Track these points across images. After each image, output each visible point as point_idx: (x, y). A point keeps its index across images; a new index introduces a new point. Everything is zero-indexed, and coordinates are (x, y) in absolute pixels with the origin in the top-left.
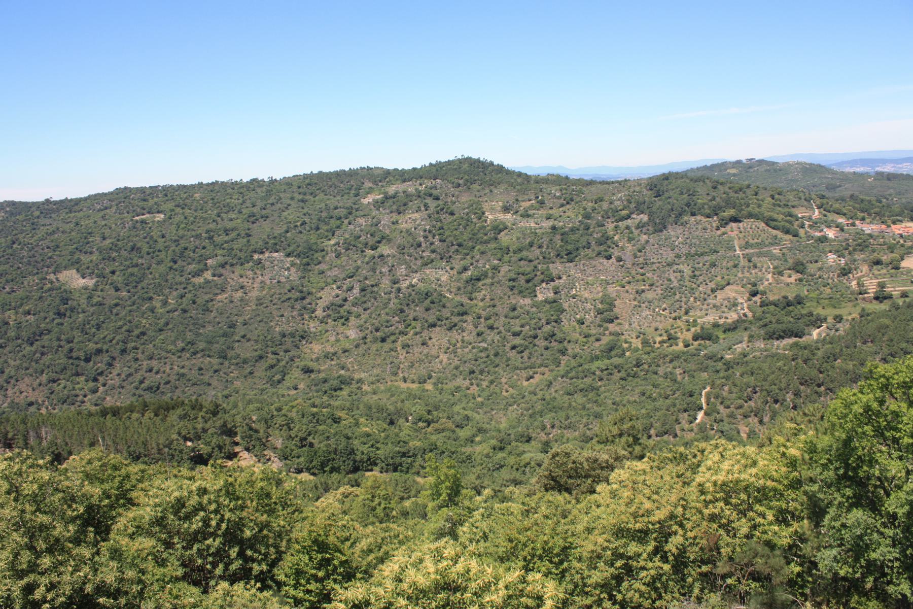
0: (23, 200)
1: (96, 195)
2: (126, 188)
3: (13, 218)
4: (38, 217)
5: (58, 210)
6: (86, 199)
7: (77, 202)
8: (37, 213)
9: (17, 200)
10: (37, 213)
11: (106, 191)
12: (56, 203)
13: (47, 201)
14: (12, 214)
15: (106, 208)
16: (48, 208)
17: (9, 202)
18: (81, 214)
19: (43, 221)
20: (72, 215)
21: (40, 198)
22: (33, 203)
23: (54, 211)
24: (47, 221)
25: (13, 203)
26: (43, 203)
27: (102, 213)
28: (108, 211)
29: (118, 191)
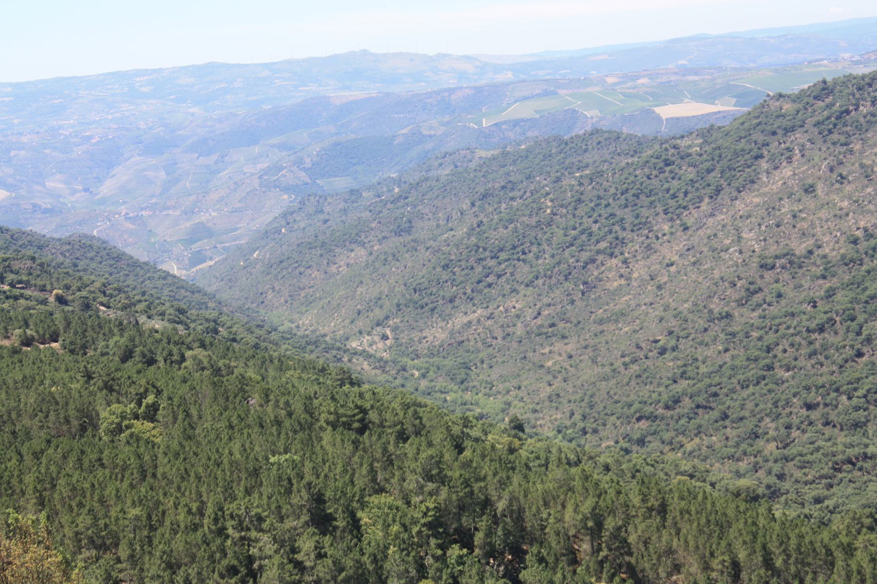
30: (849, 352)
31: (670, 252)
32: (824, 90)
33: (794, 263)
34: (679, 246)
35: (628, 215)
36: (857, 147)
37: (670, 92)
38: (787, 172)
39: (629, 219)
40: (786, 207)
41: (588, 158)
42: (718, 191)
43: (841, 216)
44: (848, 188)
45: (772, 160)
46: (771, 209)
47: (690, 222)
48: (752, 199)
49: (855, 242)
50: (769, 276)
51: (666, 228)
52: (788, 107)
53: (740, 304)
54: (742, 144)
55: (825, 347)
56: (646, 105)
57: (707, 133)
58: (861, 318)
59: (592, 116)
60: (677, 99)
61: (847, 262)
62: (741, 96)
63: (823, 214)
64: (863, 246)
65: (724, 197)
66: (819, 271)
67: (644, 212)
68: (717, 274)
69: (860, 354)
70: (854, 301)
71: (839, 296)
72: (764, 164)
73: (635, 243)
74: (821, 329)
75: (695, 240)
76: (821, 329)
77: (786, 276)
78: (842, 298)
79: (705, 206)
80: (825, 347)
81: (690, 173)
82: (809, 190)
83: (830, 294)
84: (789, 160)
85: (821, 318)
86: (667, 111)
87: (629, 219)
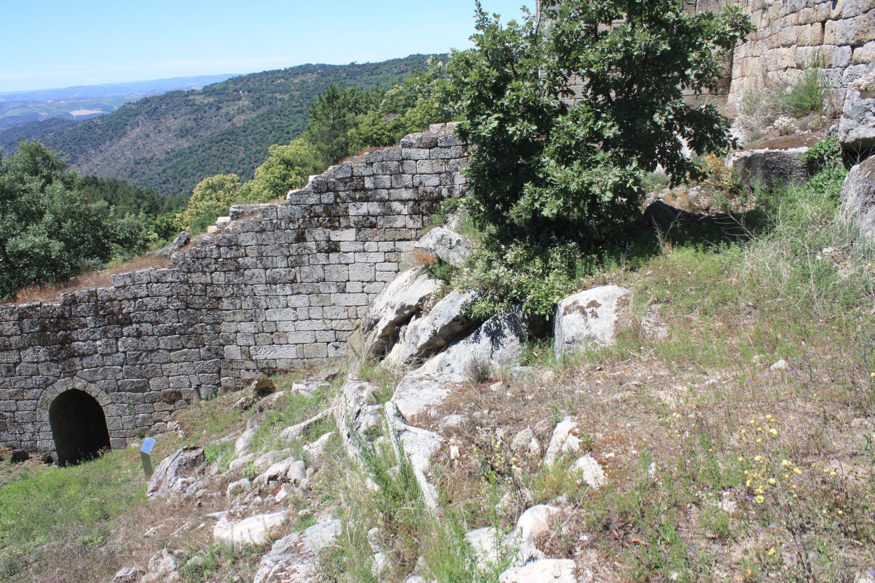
0: (332, 63)
1: (393, 60)
2: (418, 55)
3: (324, 79)
4: (345, 78)
5: (361, 73)
6: (385, 64)
7: (377, 66)
8: (344, 75)
9: (327, 63)
10: (344, 75)
11: (402, 58)
12: (359, 66)
13: (352, 64)
14: (323, 75)
15: (403, 72)
16: (353, 71)
17: (320, 65)
18: (381, 76)
19: (349, 82)
20: (374, 77)
21: (347, 62)
22: (340, 66)
23: (357, 73)
24: (353, 82)
25: (324, 66)
26: (349, 66)
27: (399, 76)
28: (404, 74)
29: (412, 58)
30: (176, 190)
31: (96, 160)
32: (146, 101)
33: (148, 162)
34: (100, 158)
35: (77, 147)
36: (163, 120)
37: (77, 107)
38: (138, 130)
39: (78, 149)
40: (140, 142)
41: (53, 128)
42: (112, 138)
43: (162, 144)
44: (162, 135)
45: (131, 126)
46: (134, 143)
47: (103, 149)
48: (125, 141)
49: (168, 153)
50: (138, 166)
51: (93, 152)
52: (133, 107)
53: (130, 177)
54: (119, 120)
55: (167, 189)
56: (66, 111)
57: (102, 117)
58: (179, 178)
59: (44, 115)
60: (79, 109)
61: (168, 160)
62: (104, 108)
63: (155, 144)
64: (172, 154)
65: (115, 140)
66: (157, 164)
67: (84, 147)
68: (117, 167)
69: (181, 190)
70: (175, 172)
71: (168, 171)
72: (129, 128)
73: (81, 158)
74: (164, 183)
75: (106, 156)
76: (164, 183)
77: (145, 166)
78: (170, 172)
79: (108, 143)
80: (167, 189)
81: (100, 132)
82: (148, 136)
83: (164, 171)
84: (138, 126)
85: (164, 179)
86: (75, 113)
87: (78, 149)
